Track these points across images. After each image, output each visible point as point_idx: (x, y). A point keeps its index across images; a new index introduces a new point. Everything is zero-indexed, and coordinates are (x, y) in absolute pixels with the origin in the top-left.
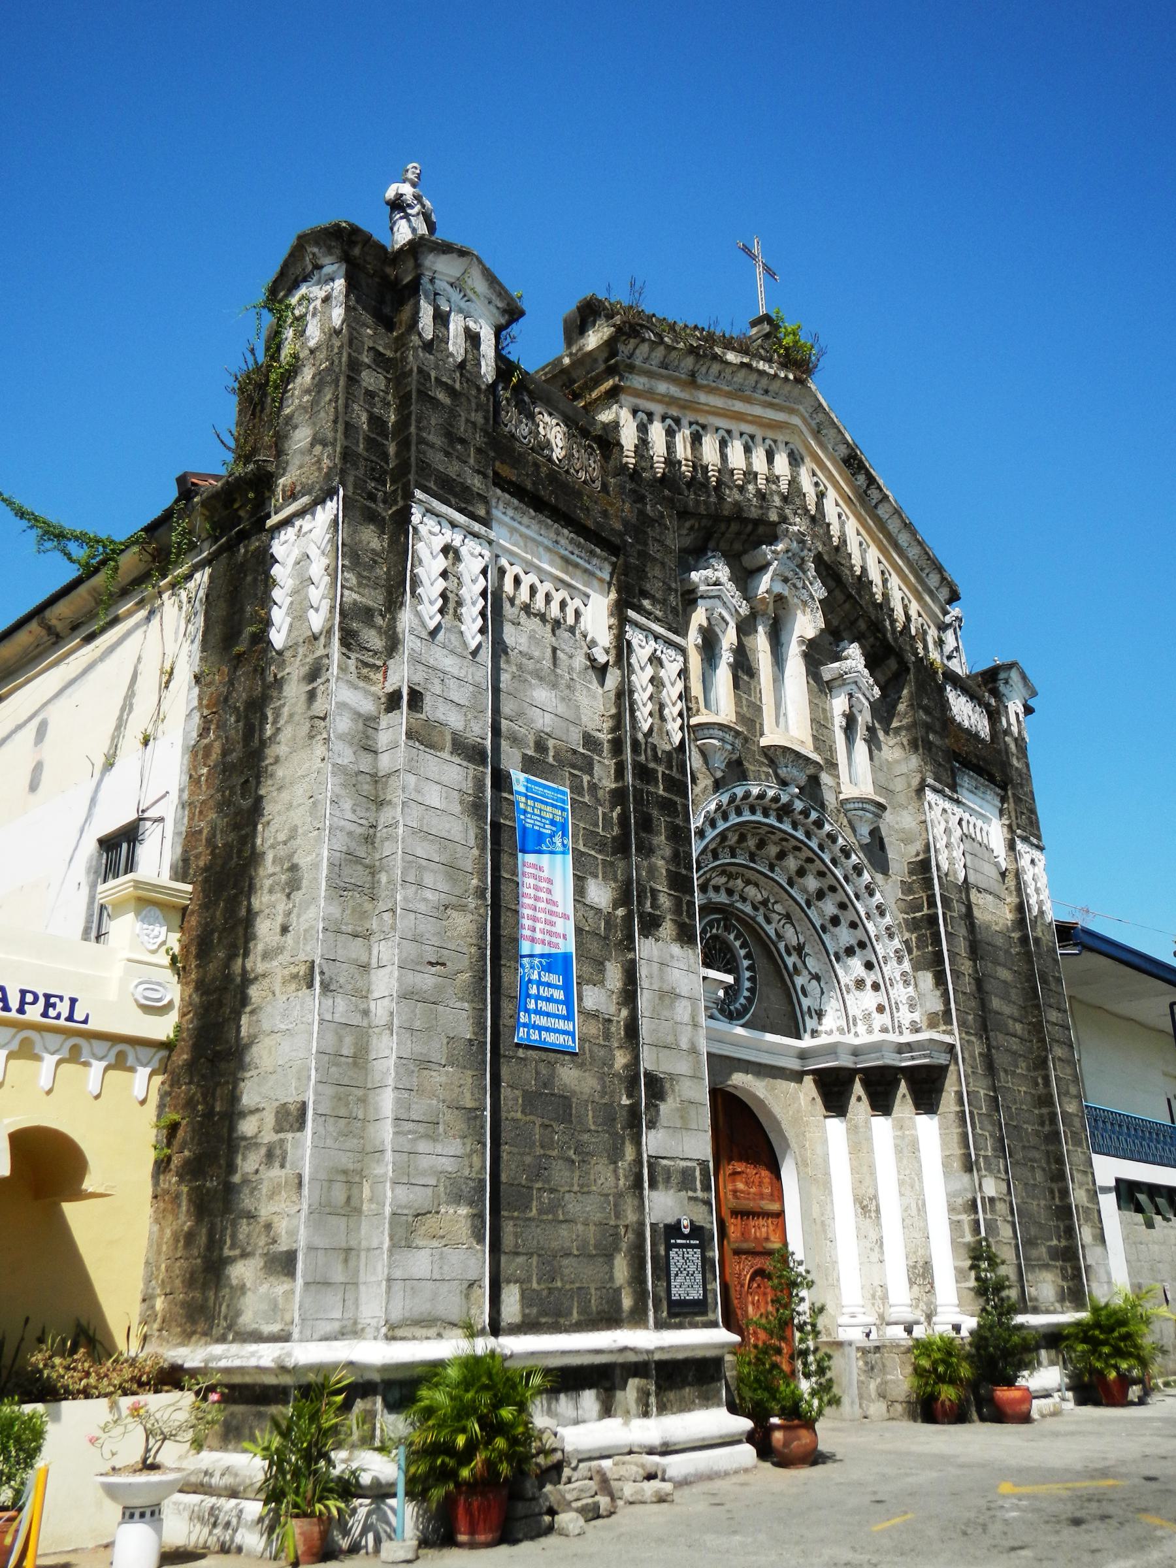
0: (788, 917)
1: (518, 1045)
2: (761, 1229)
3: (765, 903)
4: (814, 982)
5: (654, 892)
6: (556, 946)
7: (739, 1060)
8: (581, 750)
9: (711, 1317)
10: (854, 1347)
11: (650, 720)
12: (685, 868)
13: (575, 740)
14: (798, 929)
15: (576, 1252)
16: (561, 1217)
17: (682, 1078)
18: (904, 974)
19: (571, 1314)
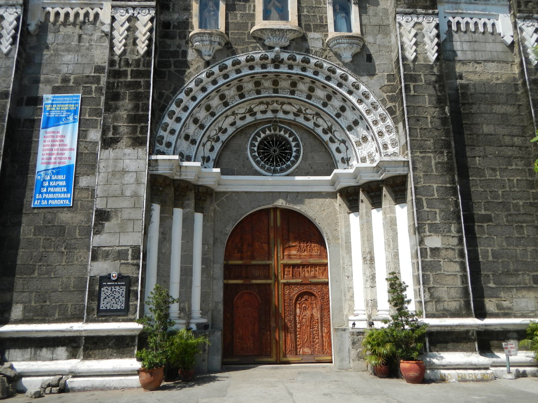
0: (318, 114)
1: (34, 208)
2: (308, 273)
3: (300, 111)
4: (342, 144)
5: (115, 128)
6: (64, 163)
7: (280, 192)
8: (93, 74)
9: (131, 317)
10: (347, 331)
11: (123, 48)
12: (142, 111)
13: (89, 72)
14: (326, 120)
15: (60, 290)
16: (53, 276)
17: (124, 209)
18: (387, 127)
19: (54, 315)
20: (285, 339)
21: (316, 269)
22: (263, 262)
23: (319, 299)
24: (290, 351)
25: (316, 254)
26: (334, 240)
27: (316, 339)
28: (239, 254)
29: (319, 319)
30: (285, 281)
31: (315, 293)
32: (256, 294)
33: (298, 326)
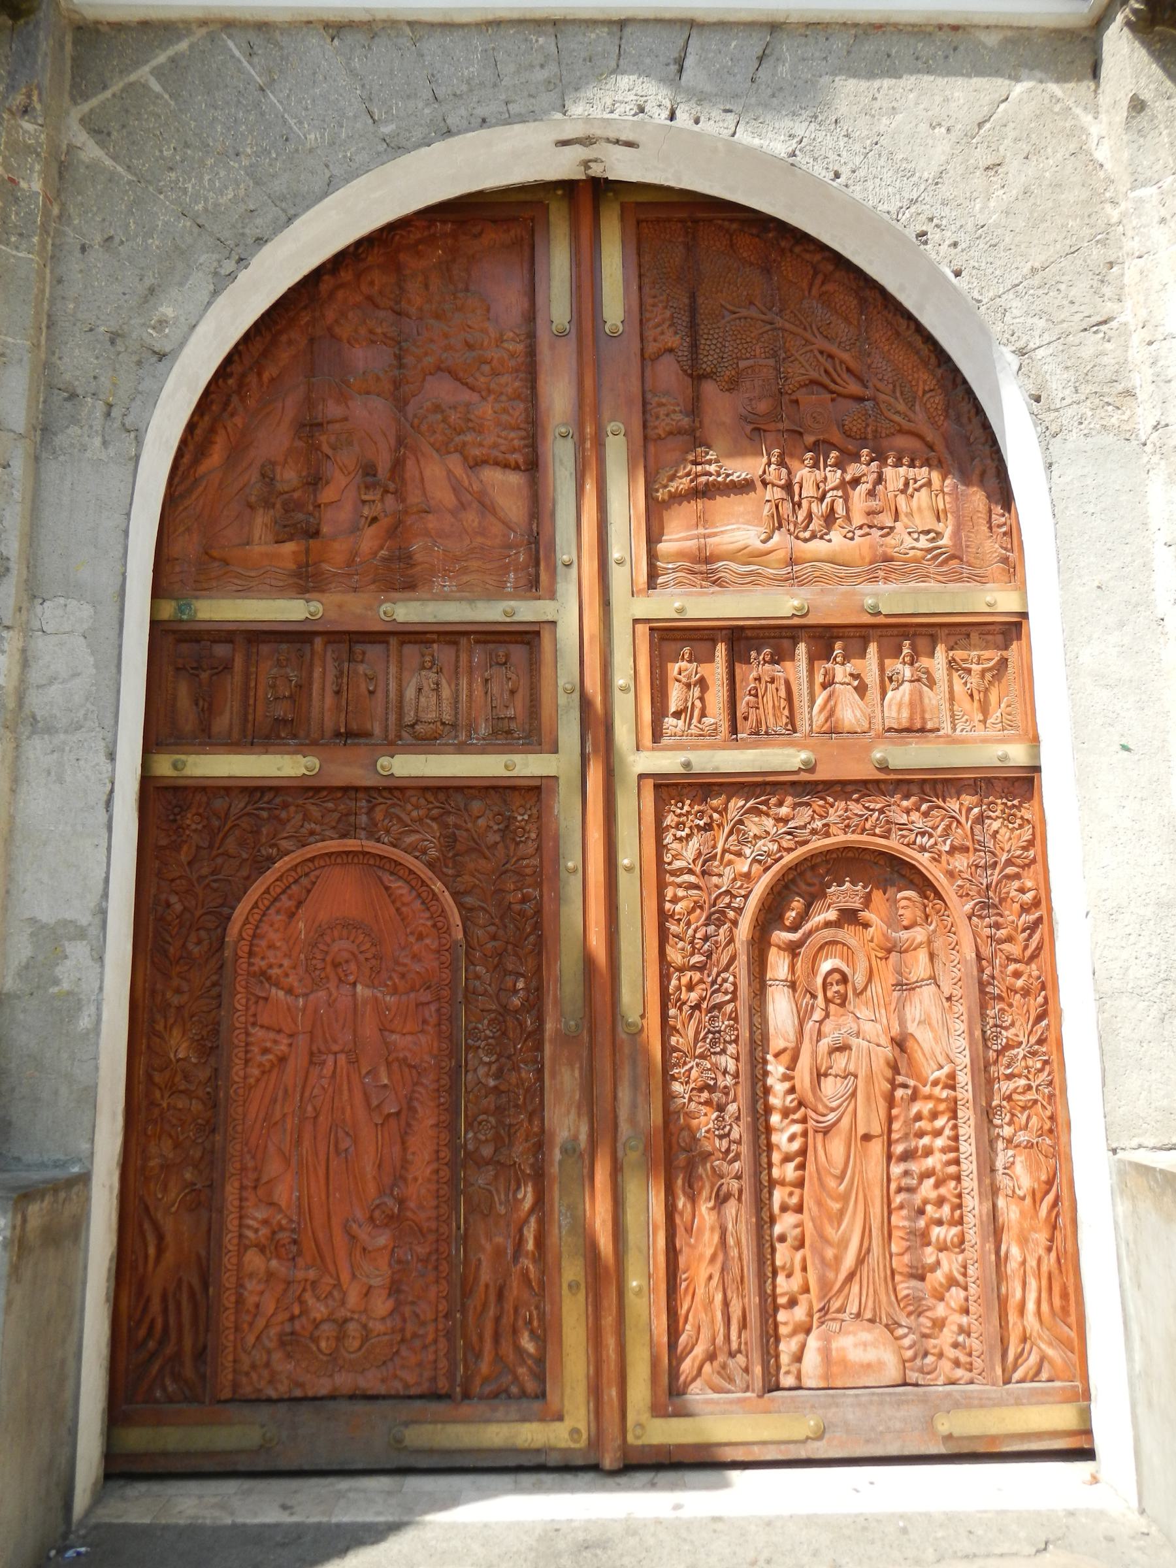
20: (672, 1252)
21: (924, 662)
22: (491, 612)
23: (961, 908)
24: (711, 1357)
25: (923, 542)
26: (1085, 409)
27: (942, 1248)
28: (289, 547)
29: (963, 1078)
30: (667, 762)
31: (923, 860)
32: (425, 873)
33: (784, 1137)
